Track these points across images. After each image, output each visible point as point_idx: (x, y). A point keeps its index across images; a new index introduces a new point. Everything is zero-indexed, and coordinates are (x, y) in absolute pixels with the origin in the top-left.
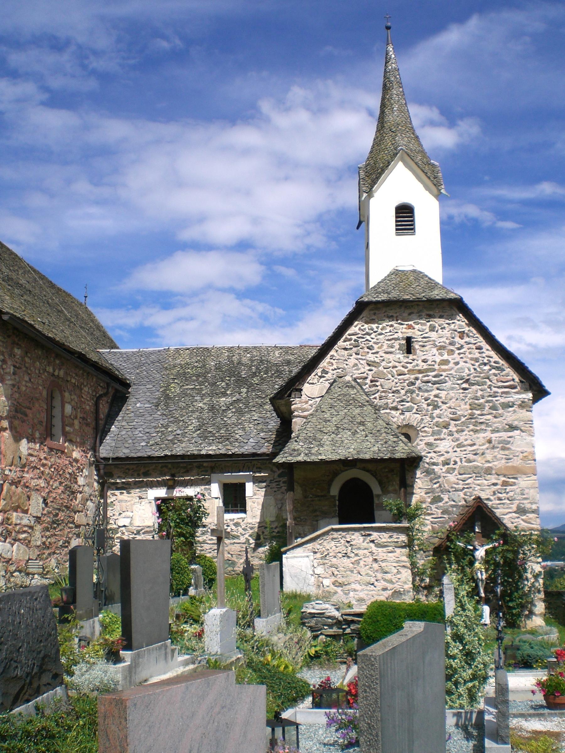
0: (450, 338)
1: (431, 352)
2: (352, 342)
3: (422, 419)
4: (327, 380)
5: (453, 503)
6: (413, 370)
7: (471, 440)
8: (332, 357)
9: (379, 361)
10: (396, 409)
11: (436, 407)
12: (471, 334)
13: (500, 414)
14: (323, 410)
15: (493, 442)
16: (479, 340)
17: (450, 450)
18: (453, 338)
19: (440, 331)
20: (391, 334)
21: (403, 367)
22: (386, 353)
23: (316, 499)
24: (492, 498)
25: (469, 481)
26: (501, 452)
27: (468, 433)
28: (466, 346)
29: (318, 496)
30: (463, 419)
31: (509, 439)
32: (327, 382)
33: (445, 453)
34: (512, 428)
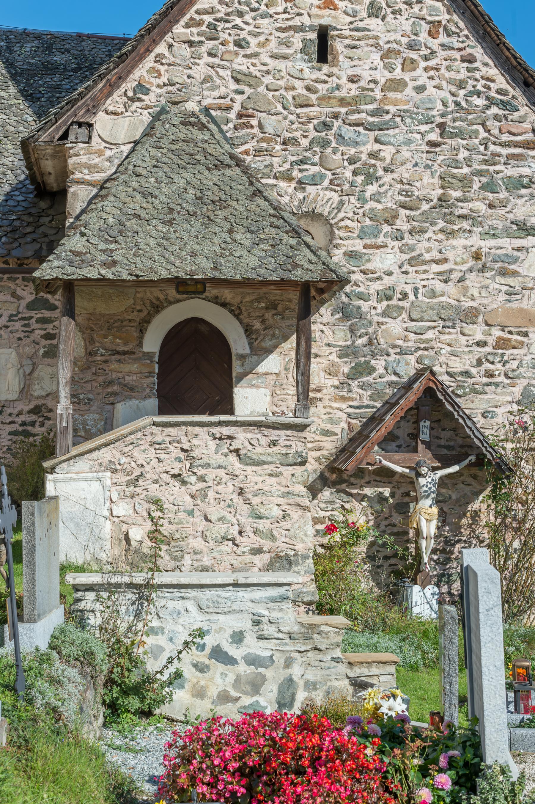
0: (409, 33)
1: (370, 61)
2: (204, 28)
3: (342, 203)
4: (147, 107)
5: (394, 378)
6: (329, 98)
7: (440, 252)
8: (159, 59)
9: (258, 74)
10: (287, 177)
11: (371, 178)
12: (454, 29)
13: (501, 201)
14: (139, 170)
15: (483, 258)
16: (468, 43)
17: (395, 269)
18: (416, 35)
19: (390, 17)
20: (286, 16)
21: (308, 89)
22: (274, 56)
23: (113, 358)
24: (474, 371)
25: (430, 334)
26: (498, 279)
27: (434, 237)
28: (442, 54)
29: (118, 353)
30: (425, 207)
31: (515, 253)
32: (145, 112)
33: (383, 275)
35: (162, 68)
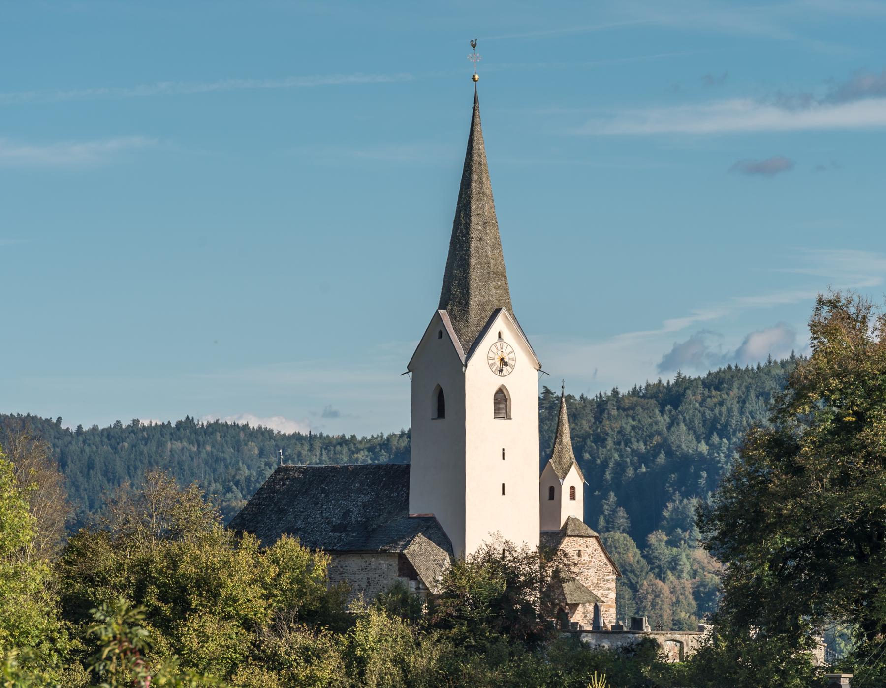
11: (587, 579)
34: (609, 589)
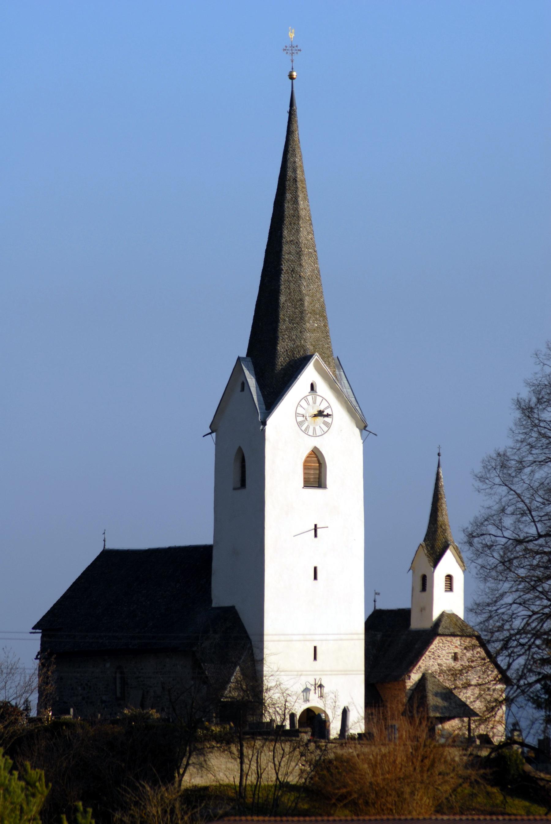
22: (446, 659)
35: (424, 662)
